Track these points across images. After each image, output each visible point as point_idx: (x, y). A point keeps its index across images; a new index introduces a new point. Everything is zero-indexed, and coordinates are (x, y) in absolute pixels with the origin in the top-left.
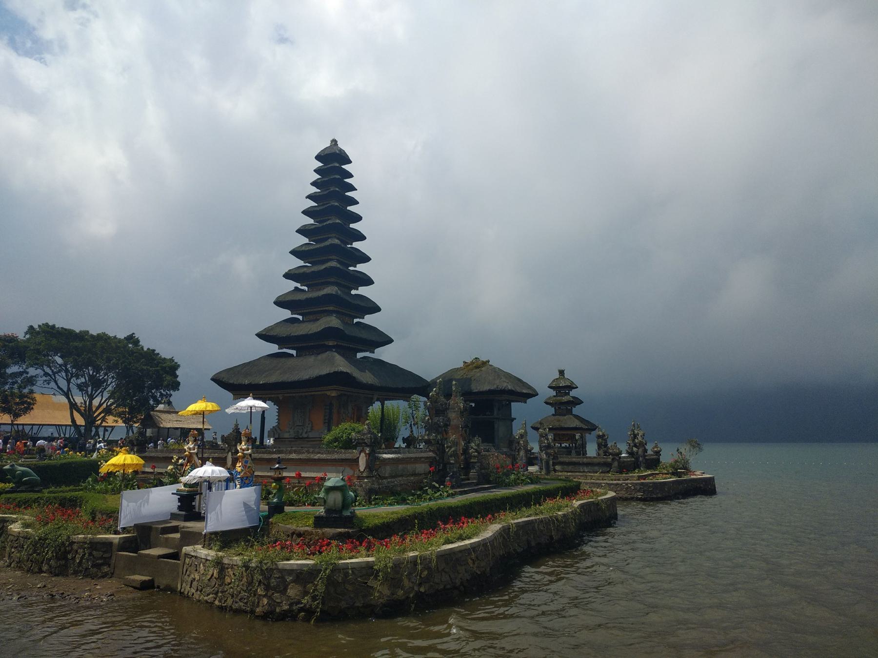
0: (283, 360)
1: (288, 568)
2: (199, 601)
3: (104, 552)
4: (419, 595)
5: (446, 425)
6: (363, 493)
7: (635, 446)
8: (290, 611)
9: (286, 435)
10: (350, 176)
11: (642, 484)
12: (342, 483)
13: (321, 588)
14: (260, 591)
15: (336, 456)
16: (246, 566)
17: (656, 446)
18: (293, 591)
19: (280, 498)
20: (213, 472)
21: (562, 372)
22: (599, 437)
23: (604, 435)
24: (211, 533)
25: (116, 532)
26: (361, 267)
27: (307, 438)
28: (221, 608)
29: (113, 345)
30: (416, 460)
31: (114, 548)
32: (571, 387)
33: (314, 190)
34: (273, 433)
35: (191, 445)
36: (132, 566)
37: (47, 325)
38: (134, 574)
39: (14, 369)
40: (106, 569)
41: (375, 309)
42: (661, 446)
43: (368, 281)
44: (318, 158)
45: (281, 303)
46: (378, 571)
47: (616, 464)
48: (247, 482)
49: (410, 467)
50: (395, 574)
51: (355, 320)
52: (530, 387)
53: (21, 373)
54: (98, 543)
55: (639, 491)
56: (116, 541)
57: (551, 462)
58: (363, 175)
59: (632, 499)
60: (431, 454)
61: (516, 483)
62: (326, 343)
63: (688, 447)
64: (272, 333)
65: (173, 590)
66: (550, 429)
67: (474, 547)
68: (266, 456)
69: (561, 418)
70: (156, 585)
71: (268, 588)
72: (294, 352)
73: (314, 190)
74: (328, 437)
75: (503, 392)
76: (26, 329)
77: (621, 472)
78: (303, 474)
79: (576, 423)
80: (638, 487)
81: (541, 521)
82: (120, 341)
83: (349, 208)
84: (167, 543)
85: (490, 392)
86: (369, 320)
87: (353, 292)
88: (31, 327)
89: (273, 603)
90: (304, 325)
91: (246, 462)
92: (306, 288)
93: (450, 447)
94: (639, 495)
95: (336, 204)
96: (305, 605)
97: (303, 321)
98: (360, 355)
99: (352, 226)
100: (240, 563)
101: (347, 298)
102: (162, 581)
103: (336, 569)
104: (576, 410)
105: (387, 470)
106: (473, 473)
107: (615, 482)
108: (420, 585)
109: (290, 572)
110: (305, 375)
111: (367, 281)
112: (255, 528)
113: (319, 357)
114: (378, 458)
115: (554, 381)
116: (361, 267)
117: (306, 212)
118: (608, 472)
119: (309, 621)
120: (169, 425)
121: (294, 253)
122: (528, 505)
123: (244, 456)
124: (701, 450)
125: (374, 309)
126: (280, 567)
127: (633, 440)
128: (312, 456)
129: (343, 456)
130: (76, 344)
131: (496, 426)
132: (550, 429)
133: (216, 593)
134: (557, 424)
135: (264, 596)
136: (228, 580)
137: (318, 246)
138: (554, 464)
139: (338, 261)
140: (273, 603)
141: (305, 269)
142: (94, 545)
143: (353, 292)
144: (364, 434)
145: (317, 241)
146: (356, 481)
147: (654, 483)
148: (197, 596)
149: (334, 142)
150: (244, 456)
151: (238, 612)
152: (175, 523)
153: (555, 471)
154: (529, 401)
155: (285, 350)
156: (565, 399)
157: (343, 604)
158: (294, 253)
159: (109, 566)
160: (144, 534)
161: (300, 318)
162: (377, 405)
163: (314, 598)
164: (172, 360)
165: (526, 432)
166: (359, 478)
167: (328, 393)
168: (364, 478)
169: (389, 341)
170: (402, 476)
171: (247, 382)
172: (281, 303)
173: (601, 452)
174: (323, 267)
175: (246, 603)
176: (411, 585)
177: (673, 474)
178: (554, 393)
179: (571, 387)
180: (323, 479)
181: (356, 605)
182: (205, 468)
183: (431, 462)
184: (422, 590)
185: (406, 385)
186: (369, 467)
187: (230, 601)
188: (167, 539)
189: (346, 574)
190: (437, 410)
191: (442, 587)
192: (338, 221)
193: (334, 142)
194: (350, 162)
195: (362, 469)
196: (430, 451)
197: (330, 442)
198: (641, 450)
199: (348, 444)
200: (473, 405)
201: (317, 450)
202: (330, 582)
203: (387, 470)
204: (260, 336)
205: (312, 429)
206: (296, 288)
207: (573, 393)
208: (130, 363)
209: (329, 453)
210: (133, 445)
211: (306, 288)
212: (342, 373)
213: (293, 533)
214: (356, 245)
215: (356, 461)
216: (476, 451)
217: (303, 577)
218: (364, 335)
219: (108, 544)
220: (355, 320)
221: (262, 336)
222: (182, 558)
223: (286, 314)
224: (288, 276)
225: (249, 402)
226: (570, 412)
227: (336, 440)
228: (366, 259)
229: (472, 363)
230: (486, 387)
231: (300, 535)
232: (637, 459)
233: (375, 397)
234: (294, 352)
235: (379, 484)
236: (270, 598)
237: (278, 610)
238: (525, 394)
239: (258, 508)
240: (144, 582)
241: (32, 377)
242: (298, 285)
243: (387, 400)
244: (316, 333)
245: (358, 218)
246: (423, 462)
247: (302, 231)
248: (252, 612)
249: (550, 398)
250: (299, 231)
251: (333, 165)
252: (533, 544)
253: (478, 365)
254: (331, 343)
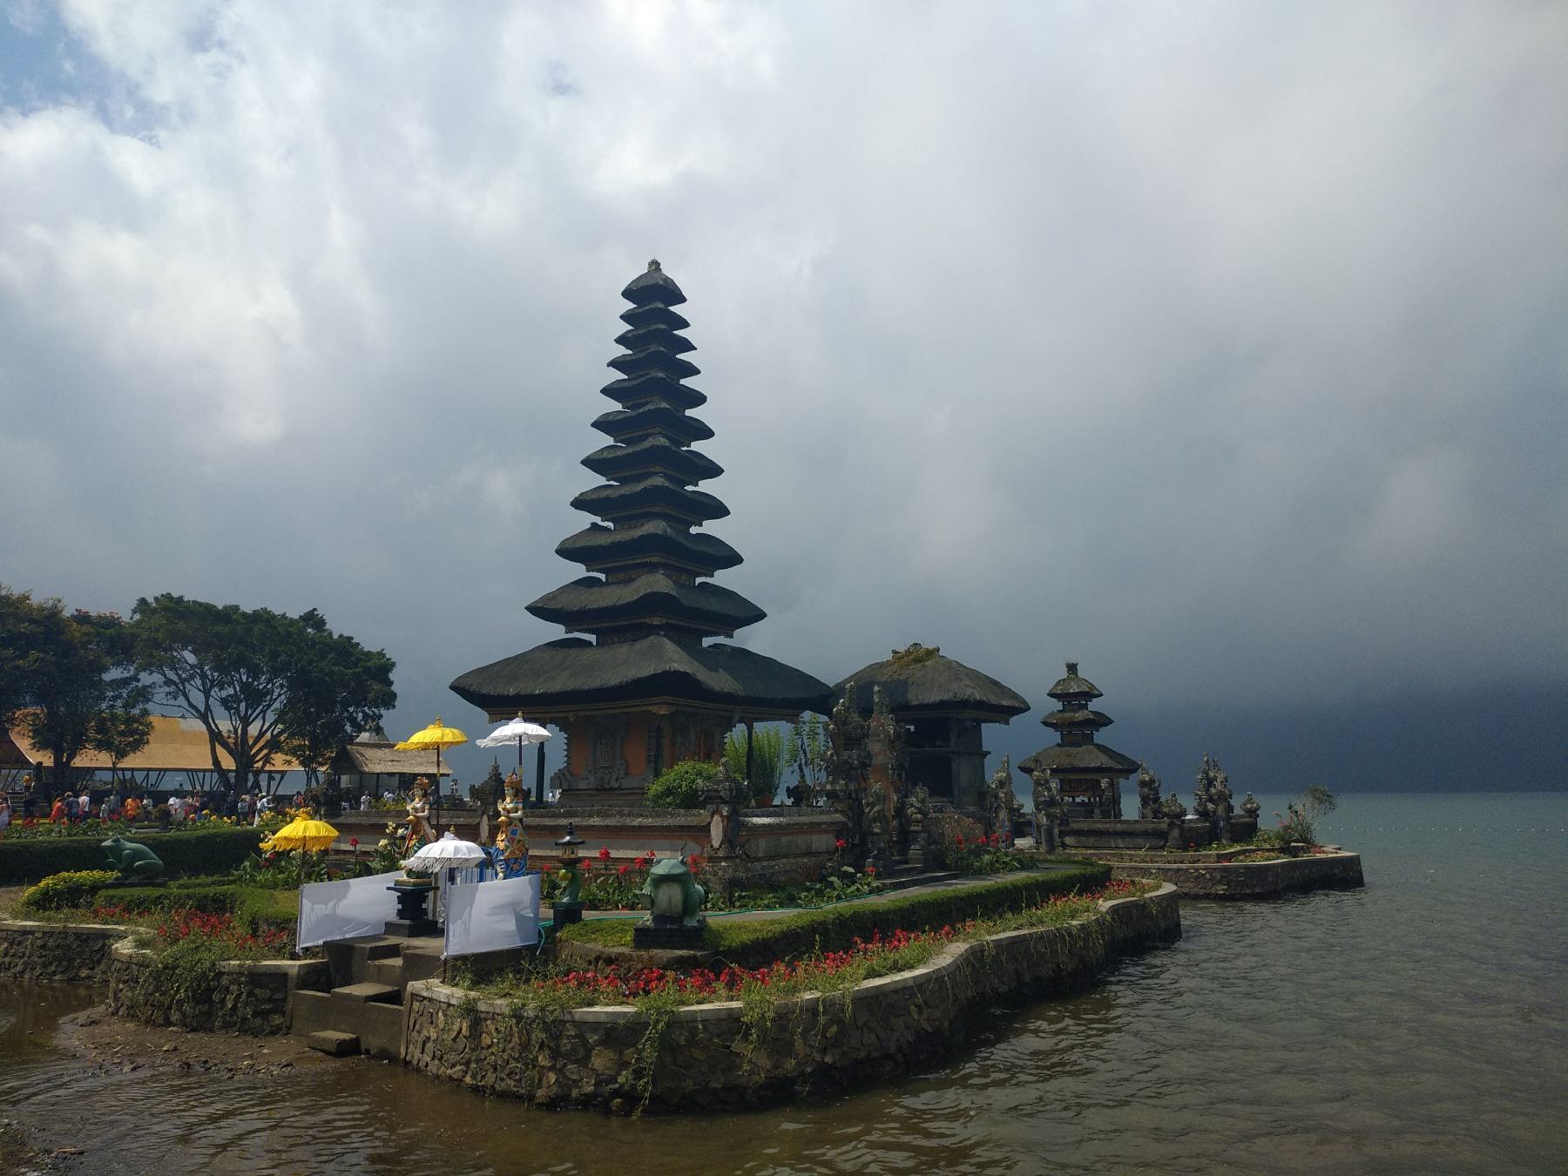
0: (573, 652)
1: (590, 1019)
2: (437, 1077)
3: (274, 991)
4: (824, 1071)
5: (864, 765)
6: (719, 887)
7: (1211, 800)
8: (594, 1095)
9: (582, 785)
10: (685, 324)
11: (1225, 869)
12: (682, 870)
13: (650, 1054)
14: (543, 1060)
15: (669, 821)
16: (517, 1015)
17: (1250, 800)
18: (601, 1061)
19: (574, 895)
20: (457, 850)
21: (1072, 668)
22: (1143, 784)
23: (1152, 781)
24: (456, 958)
25: (294, 956)
26: (706, 486)
27: (619, 788)
28: (475, 1089)
29: (281, 629)
30: (813, 828)
31: (291, 984)
32: (1090, 694)
33: (622, 351)
34: (560, 779)
35: (418, 804)
36: (323, 1015)
37: (169, 597)
38: (325, 1028)
39: (114, 674)
40: (277, 1019)
41: (733, 559)
42: (1259, 800)
43: (719, 510)
44: (628, 294)
45: (568, 551)
46: (749, 1027)
47: (1176, 833)
48: (516, 867)
49: (800, 840)
50: (778, 1032)
51: (699, 580)
52: (1015, 696)
53: (126, 682)
54: (265, 974)
55: (1219, 882)
56: (294, 971)
57: (1056, 831)
58: (706, 321)
59: (1207, 897)
60: (838, 817)
61: (993, 869)
62: (648, 621)
63: (1308, 801)
64: (552, 606)
65: (394, 1059)
66: (1053, 771)
67: (920, 984)
68: (548, 822)
69: (1073, 750)
70: (363, 1048)
71: (555, 1054)
72: (592, 638)
73: (622, 351)
74: (655, 788)
75: (964, 704)
76: (134, 604)
77: (1185, 849)
78: (614, 854)
79: (1102, 760)
81: (1041, 937)
82: (292, 622)
83: (683, 382)
84: (379, 976)
85: (942, 704)
86: (723, 578)
87: (694, 530)
88: (143, 601)
89: (565, 1083)
90: (609, 590)
91: (514, 832)
92: (610, 525)
93: (873, 805)
94: (1221, 889)
95: (661, 375)
96: (622, 1086)
97: (607, 584)
98: (707, 642)
99: (688, 413)
100: (507, 1011)
101: (681, 540)
102: (373, 1042)
103: (675, 1022)
104: (1101, 736)
105: (761, 846)
106: (915, 850)
107: (1175, 866)
108: (824, 1051)
109: (595, 1026)
110: (613, 678)
111: (718, 510)
112: (531, 949)
113: (638, 645)
114: (744, 825)
115: (1058, 683)
116: (706, 486)
117: (608, 391)
118: (1162, 848)
119: (628, 1114)
120: (378, 769)
121: (587, 462)
122: (1016, 908)
123: (510, 821)
124: (1333, 807)
125: (732, 559)
126: (577, 1017)
127: (1207, 790)
128: (628, 821)
129: (682, 821)
130: (219, 628)
131: (954, 767)
132: (1053, 771)
133: (467, 1064)
134: (1066, 762)
135: (550, 1069)
136: (486, 1040)
137: (630, 450)
138: (1062, 834)
139: (668, 477)
140: (565, 1083)
141: (609, 492)
142: (258, 979)
143: (694, 530)
144: (718, 782)
145: (628, 442)
146: (707, 866)
147: (1247, 868)
148: (433, 1067)
149: (655, 265)
150: (510, 821)
151: (504, 1096)
152: (392, 940)
153: (1064, 846)
154: (1013, 720)
155: (577, 635)
156: (1080, 716)
157: (689, 1085)
158: (589, 462)
159: (283, 1013)
160: (341, 960)
161: (602, 577)
162: (740, 729)
163: (638, 1074)
164: (381, 654)
165: (1009, 777)
166: (711, 859)
167: (654, 709)
168: (721, 859)
169: (759, 615)
170: (787, 856)
171: (512, 691)
172: (568, 551)
173: (1148, 812)
174: (640, 486)
175: (519, 1081)
176: (808, 1051)
177: (1282, 850)
178: (1059, 706)
179: (1090, 694)
180: (648, 862)
181: (712, 1085)
182: (442, 843)
183: (839, 831)
184: (828, 1059)
185: (790, 693)
186: (728, 840)
187: (491, 1078)
188: (380, 967)
189: (693, 1031)
190: (847, 738)
191: (863, 1054)
192: (664, 405)
193: (655, 265)
194: (682, 299)
195: (716, 844)
196: (837, 811)
197: (659, 797)
198: (1221, 810)
199: (691, 800)
200: (912, 728)
201: (636, 811)
202: (666, 1044)
203: (761, 846)
204: (534, 610)
205: (627, 774)
206: (594, 525)
207: (1094, 705)
208: (311, 662)
209: (658, 815)
210: (319, 804)
211: (610, 525)
212: (677, 672)
213: (598, 959)
214: (697, 446)
215: (706, 829)
216: (920, 811)
217: (618, 1035)
218: (713, 605)
219: (281, 977)
220: (699, 580)
221: (537, 610)
222: (407, 1001)
223: (578, 571)
224: (579, 504)
225: (516, 728)
226: (1089, 739)
227: (669, 792)
228: (714, 471)
229: (908, 652)
230: (934, 697)
231: (609, 961)
232: (1215, 824)
233: (737, 718)
234: (592, 638)
235: (748, 870)
236: (560, 1072)
237: (575, 1093)
238: (1007, 708)
239: (536, 914)
240: (342, 1043)
241: (145, 687)
242: (598, 520)
243: (757, 720)
244: (630, 605)
245: (699, 399)
246: (826, 832)
247: (602, 424)
248: (531, 1097)
249: (1052, 714)
250: (596, 425)
251: (654, 306)
252: (1027, 978)
253: (920, 656)
254: (656, 621)
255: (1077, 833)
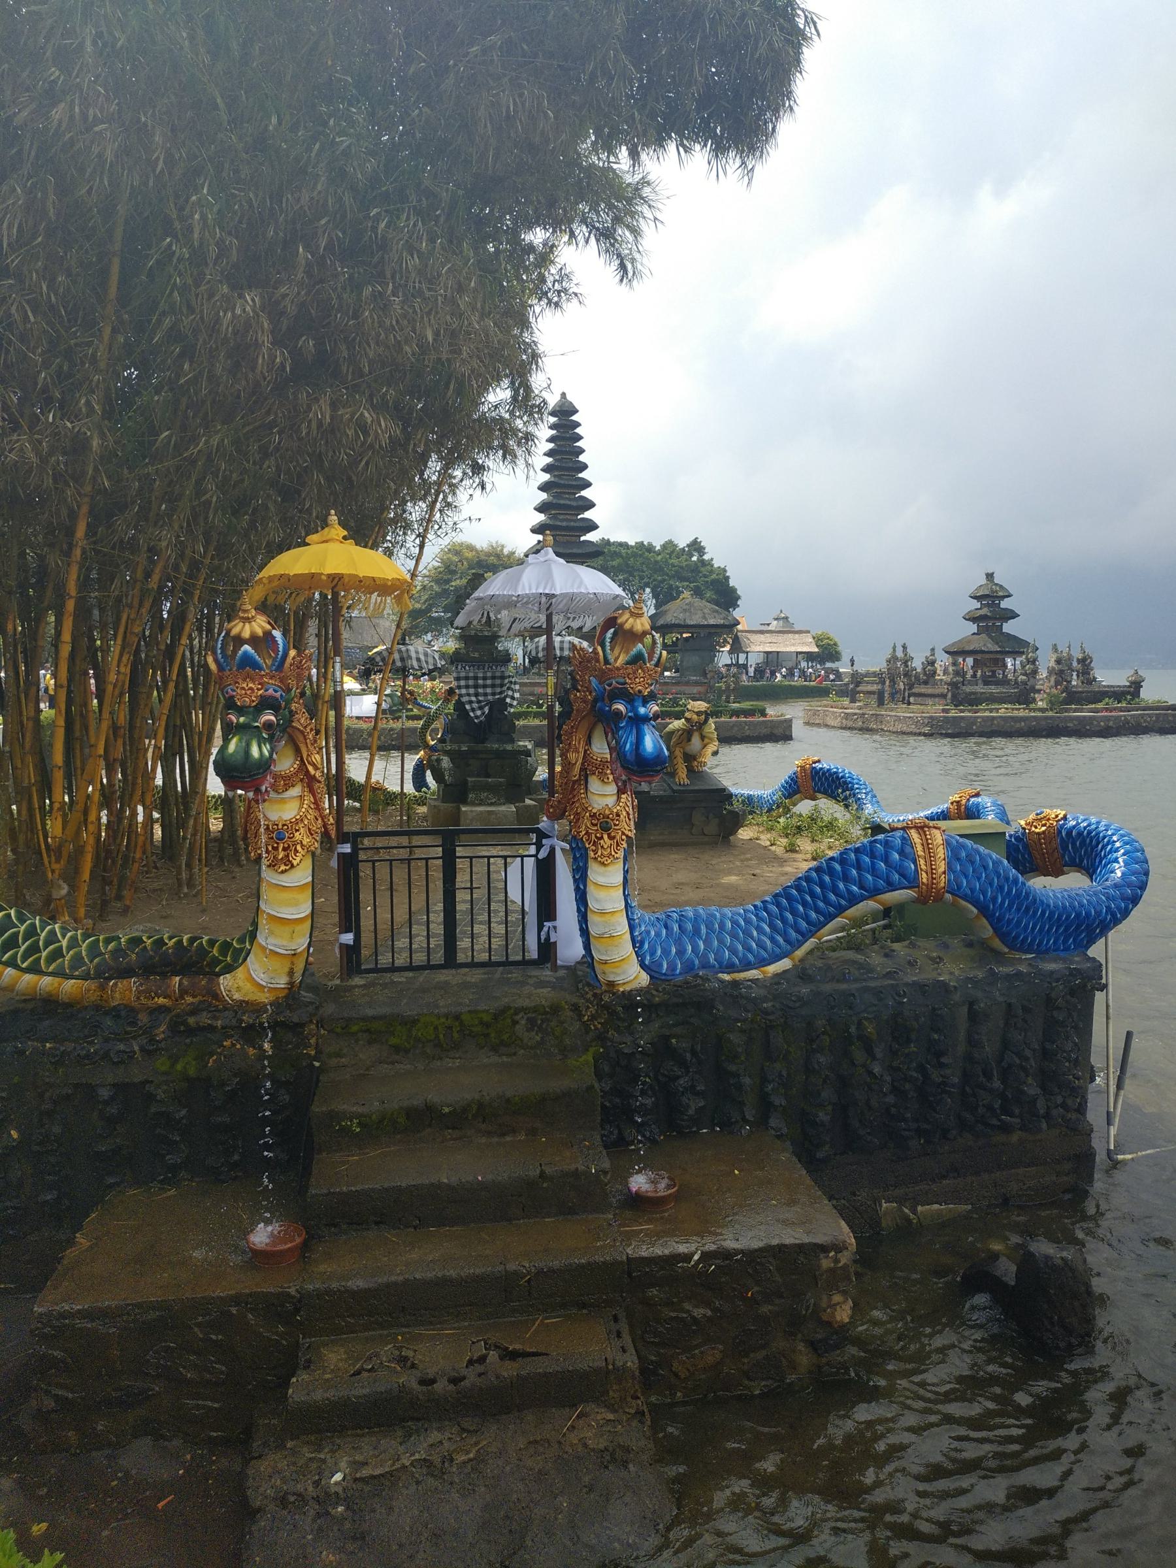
21: (990, 576)
47: (950, 695)
59: (920, 734)
80: (926, 721)
87: (582, 538)
94: (927, 730)
99: (580, 475)
104: (1009, 627)
116: (587, 515)
143: (582, 538)
149: (563, 395)
193: (563, 395)
207: (1004, 604)
255: (915, 695)
